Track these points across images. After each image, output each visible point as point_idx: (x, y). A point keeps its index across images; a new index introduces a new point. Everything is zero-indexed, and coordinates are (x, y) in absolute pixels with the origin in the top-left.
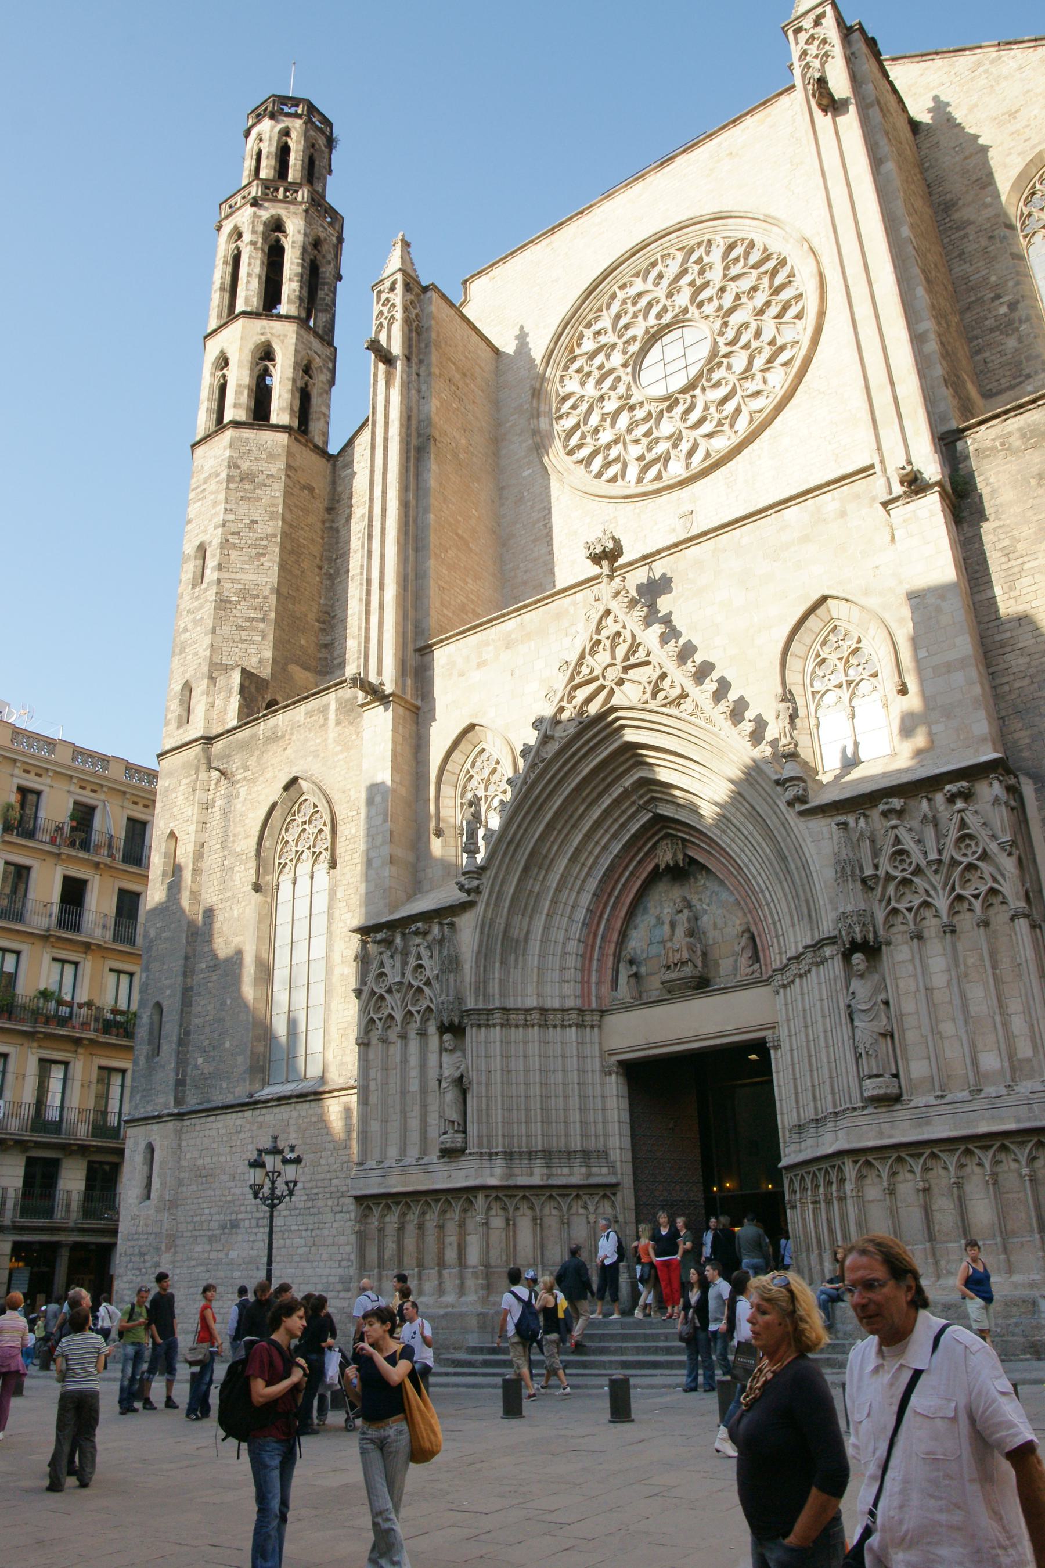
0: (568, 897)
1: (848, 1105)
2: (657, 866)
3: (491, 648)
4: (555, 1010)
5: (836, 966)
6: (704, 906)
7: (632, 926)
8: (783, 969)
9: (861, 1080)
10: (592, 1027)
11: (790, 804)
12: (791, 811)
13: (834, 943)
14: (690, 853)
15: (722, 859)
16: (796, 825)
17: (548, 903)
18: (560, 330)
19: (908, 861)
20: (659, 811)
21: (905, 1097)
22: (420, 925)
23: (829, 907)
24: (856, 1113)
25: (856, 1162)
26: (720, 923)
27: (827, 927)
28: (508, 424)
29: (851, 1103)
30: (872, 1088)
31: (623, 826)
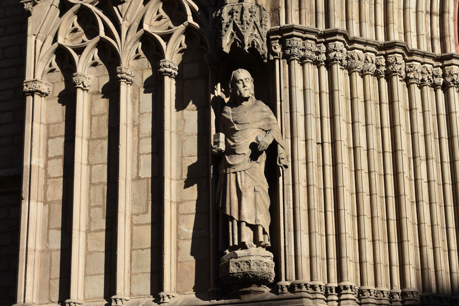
4: (424, 55)
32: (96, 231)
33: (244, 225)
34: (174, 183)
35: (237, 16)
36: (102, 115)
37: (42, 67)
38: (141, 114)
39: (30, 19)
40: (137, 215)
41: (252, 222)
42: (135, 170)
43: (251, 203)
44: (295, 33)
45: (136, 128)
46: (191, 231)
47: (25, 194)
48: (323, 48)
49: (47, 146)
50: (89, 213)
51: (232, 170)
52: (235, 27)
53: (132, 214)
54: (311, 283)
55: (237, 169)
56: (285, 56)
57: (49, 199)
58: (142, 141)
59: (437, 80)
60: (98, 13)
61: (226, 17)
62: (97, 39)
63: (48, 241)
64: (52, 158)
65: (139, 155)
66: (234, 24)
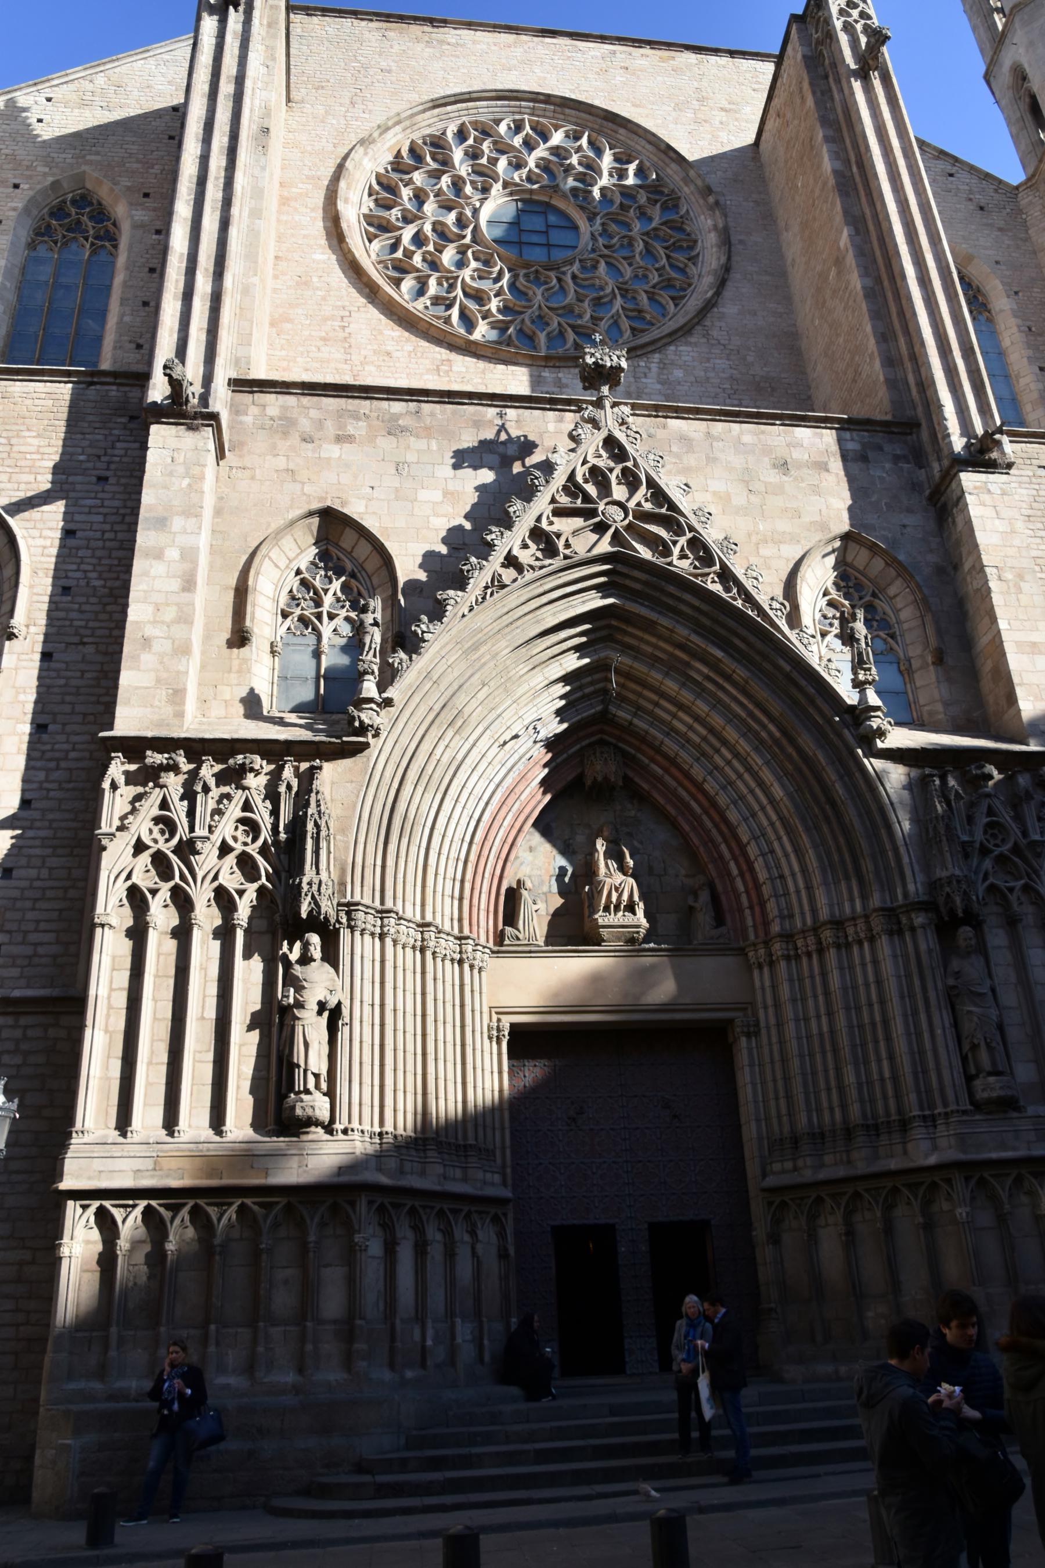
1: (953, 1107)
3: (362, 424)
6: (636, 843)
9: (969, 1079)
10: (480, 970)
13: (926, 910)
14: (631, 774)
15: (680, 790)
18: (390, 123)
19: (1000, 837)
21: (1022, 1103)
22: (257, 758)
23: (916, 867)
24: (965, 1118)
25: (967, 1179)
28: (294, 190)
30: (988, 1088)
32: (157, 1064)
33: (309, 1073)
34: (238, 1026)
35: (315, 887)
36: (170, 954)
37: (113, 901)
38: (208, 959)
39: (104, 854)
40: (200, 1052)
41: (316, 1071)
42: (200, 1010)
43: (316, 1054)
44: (360, 907)
45: (203, 972)
46: (251, 1072)
47: (89, 1021)
48: (379, 921)
49: (112, 977)
50: (152, 1046)
51: (301, 1023)
52: (313, 897)
53: (195, 1052)
54: (360, 1128)
55: (305, 1022)
56: (350, 926)
57: (110, 1029)
58: (208, 984)
60: (174, 859)
61: (305, 887)
62: (171, 884)
63: (107, 1068)
64: (115, 990)
65: (204, 996)
66: (313, 895)
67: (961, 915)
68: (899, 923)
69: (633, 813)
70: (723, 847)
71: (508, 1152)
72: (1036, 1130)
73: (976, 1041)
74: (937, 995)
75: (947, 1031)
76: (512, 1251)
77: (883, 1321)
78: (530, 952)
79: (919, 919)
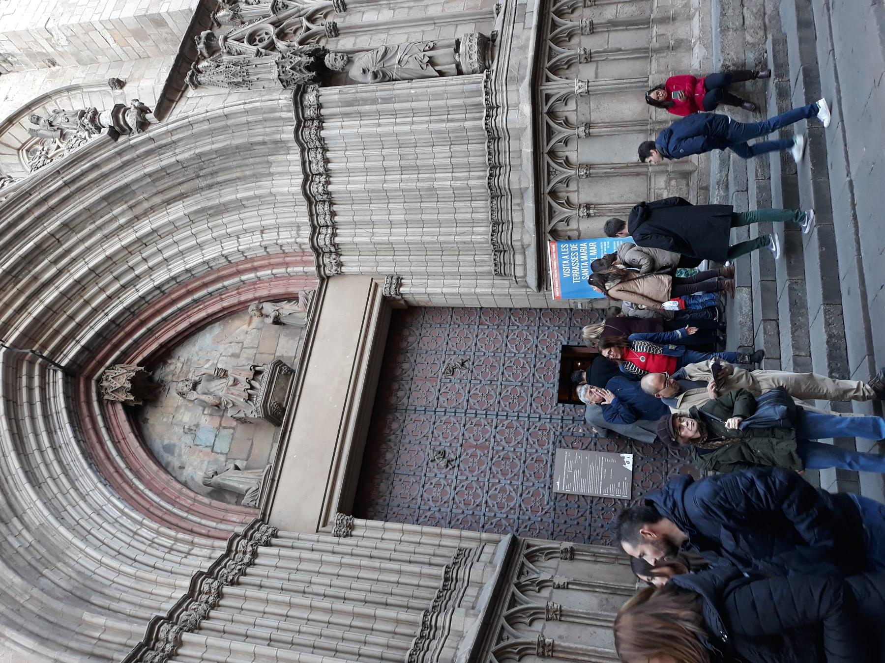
0: (79, 511)
2: (125, 404)
5: (330, 93)
7: (177, 473)
8: (314, 228)
10: (275, 535)
11: (143, 125)
12: (150, 128)
13: (305, 92)
16: (168, 125)
17: (62, 530)
19: (264, 35)
20: (63, 364)
24: (493, 77)
25: (548, 80)
26: (235, 348)
27: (284, 98)
29: (480, 83)
30: (470, 57)
31: (46, 416)
59: (246, 560)
67: (312, 59)
68: (312, 119)
69: (179, 365)
70: (226, 283)
71: (466, 533)
72: (514, 23)
73: (427, 59)
74: (381, 90)
75: (413, 86)
76: (568, 545)
77: (673, 182)
78: (273, 480)
79: (310, 98)
